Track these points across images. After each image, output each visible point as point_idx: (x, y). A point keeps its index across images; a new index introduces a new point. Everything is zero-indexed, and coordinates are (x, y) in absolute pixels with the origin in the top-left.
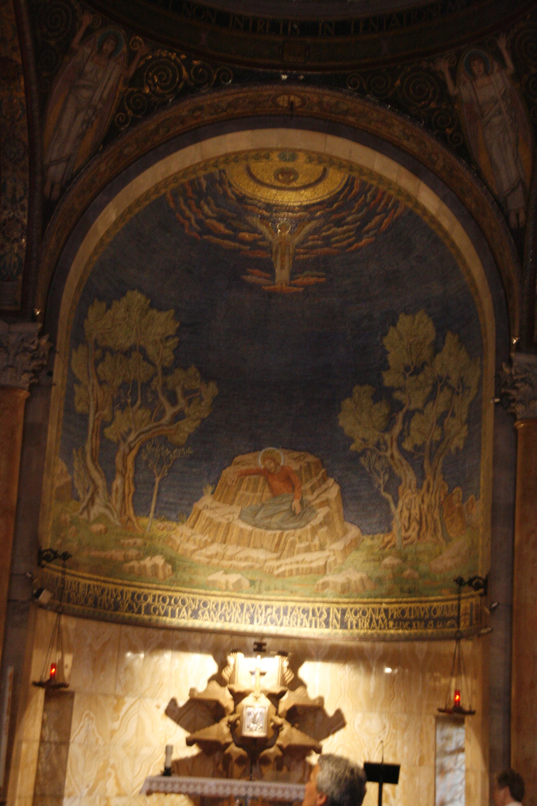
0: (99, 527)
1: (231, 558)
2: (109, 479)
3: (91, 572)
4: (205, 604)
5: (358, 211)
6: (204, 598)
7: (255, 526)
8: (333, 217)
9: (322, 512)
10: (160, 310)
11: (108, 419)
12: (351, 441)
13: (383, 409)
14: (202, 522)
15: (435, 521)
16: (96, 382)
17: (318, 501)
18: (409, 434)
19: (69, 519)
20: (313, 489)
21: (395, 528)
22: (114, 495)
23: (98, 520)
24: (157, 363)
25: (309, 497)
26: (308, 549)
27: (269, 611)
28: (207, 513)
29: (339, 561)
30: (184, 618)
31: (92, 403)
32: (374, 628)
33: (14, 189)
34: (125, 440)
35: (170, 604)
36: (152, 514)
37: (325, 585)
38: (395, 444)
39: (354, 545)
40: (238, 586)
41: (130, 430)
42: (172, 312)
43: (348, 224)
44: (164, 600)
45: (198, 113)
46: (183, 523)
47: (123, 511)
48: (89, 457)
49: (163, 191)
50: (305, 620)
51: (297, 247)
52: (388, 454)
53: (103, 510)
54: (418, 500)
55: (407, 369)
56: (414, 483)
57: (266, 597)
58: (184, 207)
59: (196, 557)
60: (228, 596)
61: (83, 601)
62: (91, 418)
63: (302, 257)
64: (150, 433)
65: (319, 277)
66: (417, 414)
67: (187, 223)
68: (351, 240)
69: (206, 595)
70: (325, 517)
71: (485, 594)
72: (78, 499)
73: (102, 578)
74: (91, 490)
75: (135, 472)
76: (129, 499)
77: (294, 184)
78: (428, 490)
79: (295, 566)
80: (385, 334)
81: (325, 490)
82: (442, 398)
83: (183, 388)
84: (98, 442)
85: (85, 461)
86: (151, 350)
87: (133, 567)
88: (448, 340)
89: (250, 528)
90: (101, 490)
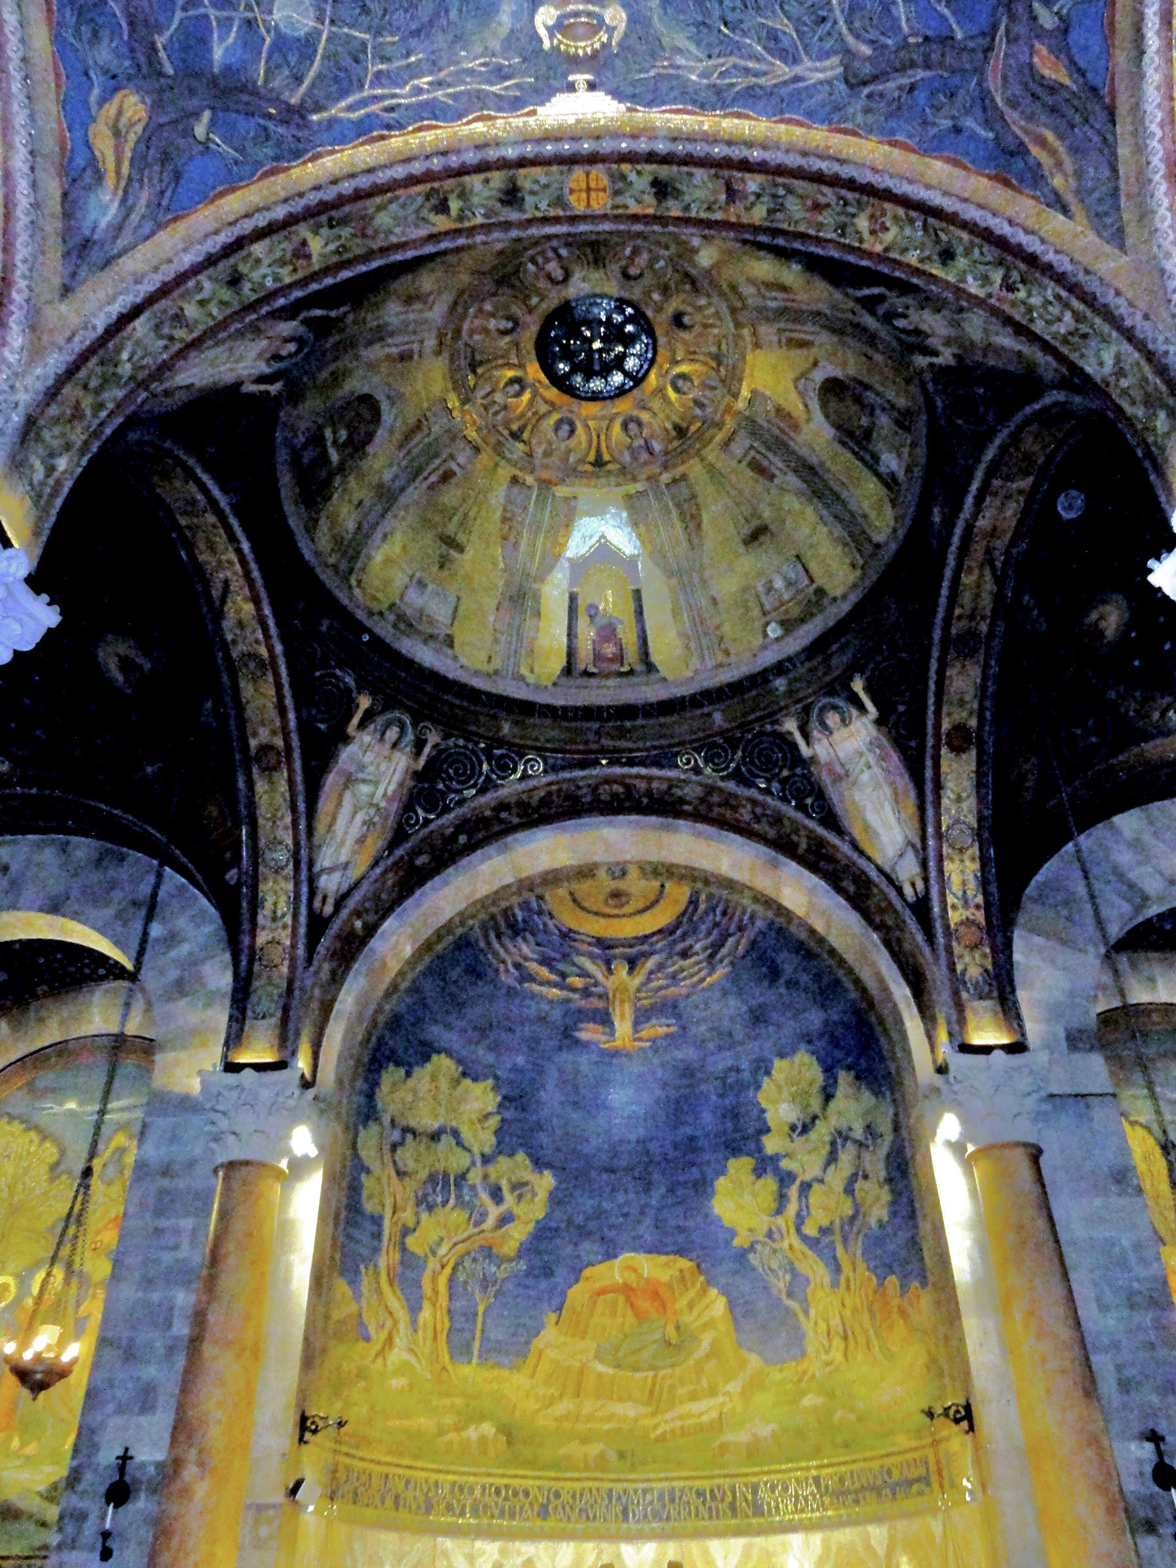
0: (402, 1382)
1: (589, 1419)
2: (414, 1309)
3: (390, 1453)
4: (557, 1495)
5: (709, 934)
6: (555, 1485)
7: (618, 1366)
8: (680, 947)
9: (706, 1340)
10: (475, 1080)
11: (411, 1225)
12: (733, 1233)
13: (769, 1184)
14: (544, 1367)
15: (866, 1332)
16: (393, 1173)
17: (698, 1323)
18: (809, 1213)
19: (354, 1371)
20: (691, 1306)
21: (810, 1350)
22: (421, 1333)
23: (399, 1371)
24: (476, 1150)
25: (687, 1318)
26: (693, 1397)
27: (648, 1497)
28: (551, 1354)
29: (739, 1409)
30: (528, 1519)
31: (389, 1202)
32: (802, 1511)
33: (275, 904)
34: (434, 1253)
35: (506, 1498)
36: (475, 1360)
37: (724, 1448)
38: (793, 1230)
39: (756, 1384)
40: (601, 1463)
41: (442, 1239)
42: (490, 1082)
43: (697, 954)
44: (498, 1492)
45: (503, 815)
46: (518, 1369)
47: (435, 1357)
48: (384, 1278)
49: (471, 922)
50: (701, 1507)
51: (638, 990)
52: (786, 1244)
53: (406, 1356)
54: (837, 1304)
55: (793, 1128)
56: (827, 1280)
57: (641, 1476)
58: (497, 946)
59: (541, 1422)
60: (588, 1479)
61: (377, 1500)
62: (387, 1223)
63: (645, 1002)
64: (468, 1243)
65: (668, 1026)
66: (816, 1186)
67: (502, 967)
68: (702, 974)
69: (557, 1479)
70: (712, 1345)
71: (972, 1428)
72: (367, 1339)
73: (406, 1462)
74: (389, 1323)
75: (450, 1299)
76: (443, 1338)
77: (627, 910)
78: (848, 1288)
79: (679, 1423)
80: (758, 1087)
81: (707, 1306)
82: (846, 1157)
83: (509, 1180)
84: (397, 1256)
85: (378, 1283)
86: (466, 1134)
87: (451, 1442)
88: (841, 1081)
89: (611, 1371)
90: (402, 1326)
